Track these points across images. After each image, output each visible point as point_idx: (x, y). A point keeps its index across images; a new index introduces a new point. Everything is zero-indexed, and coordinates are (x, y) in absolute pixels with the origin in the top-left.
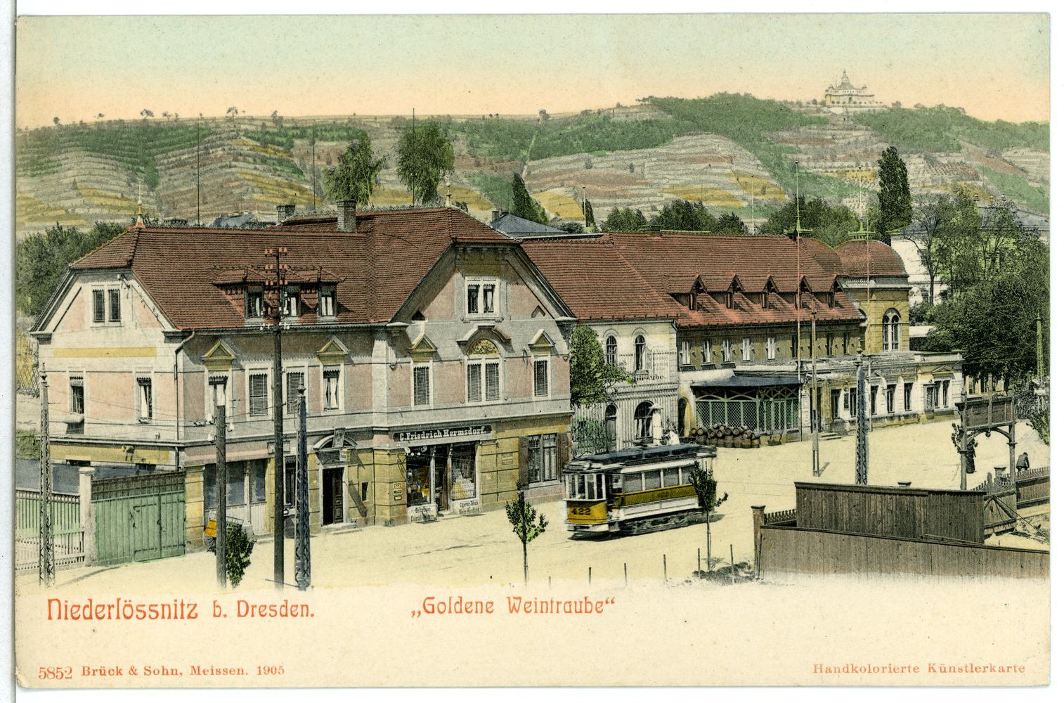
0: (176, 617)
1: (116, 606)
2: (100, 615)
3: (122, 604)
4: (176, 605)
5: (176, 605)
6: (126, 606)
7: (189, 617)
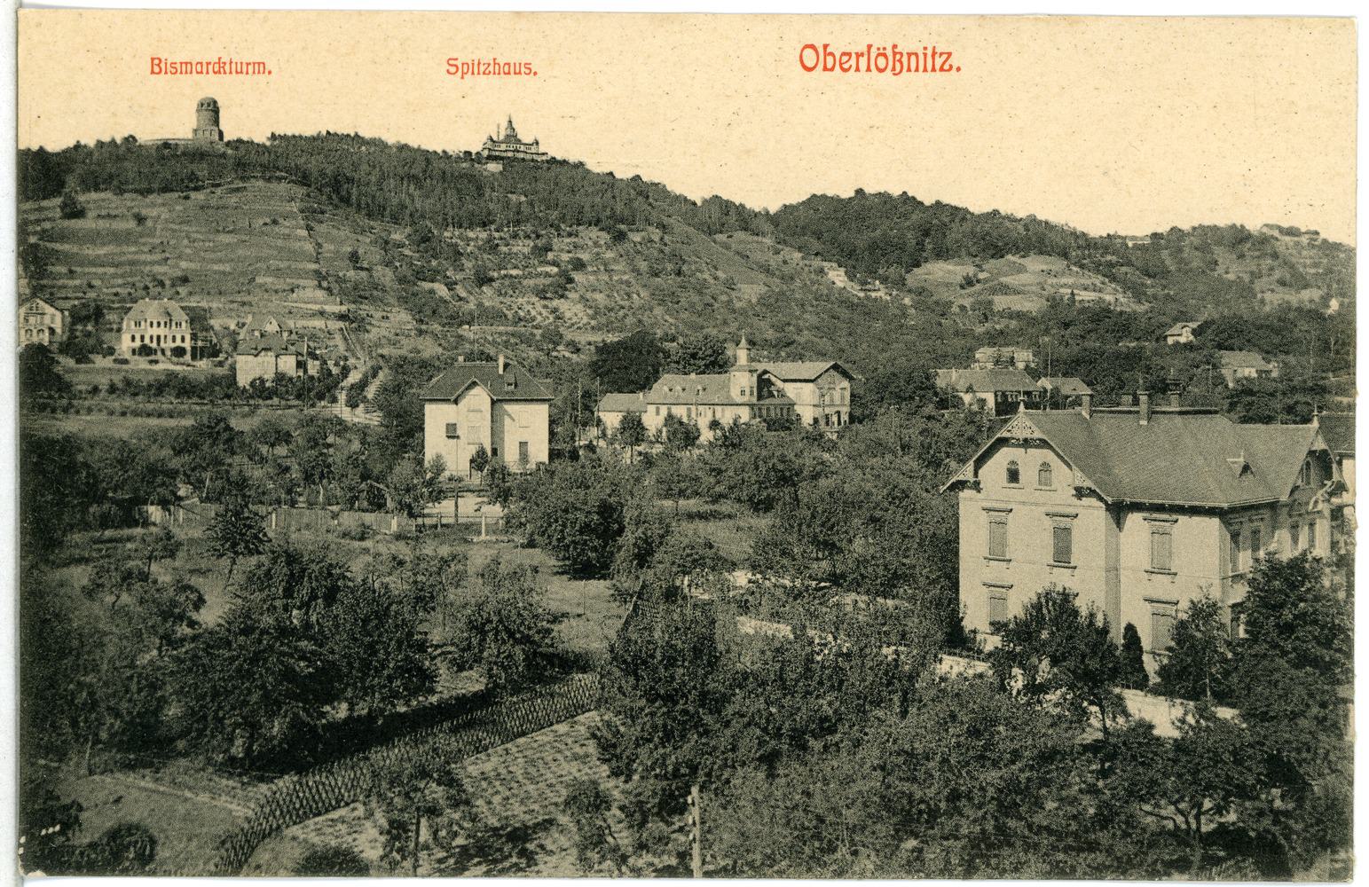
0: (925, 70)
1: (866, 57)
2: (846, 66)
3: (874, 52)
4: (925, 55)
5: (925, 55)
6: (879, 55)
7: (942, 69)
